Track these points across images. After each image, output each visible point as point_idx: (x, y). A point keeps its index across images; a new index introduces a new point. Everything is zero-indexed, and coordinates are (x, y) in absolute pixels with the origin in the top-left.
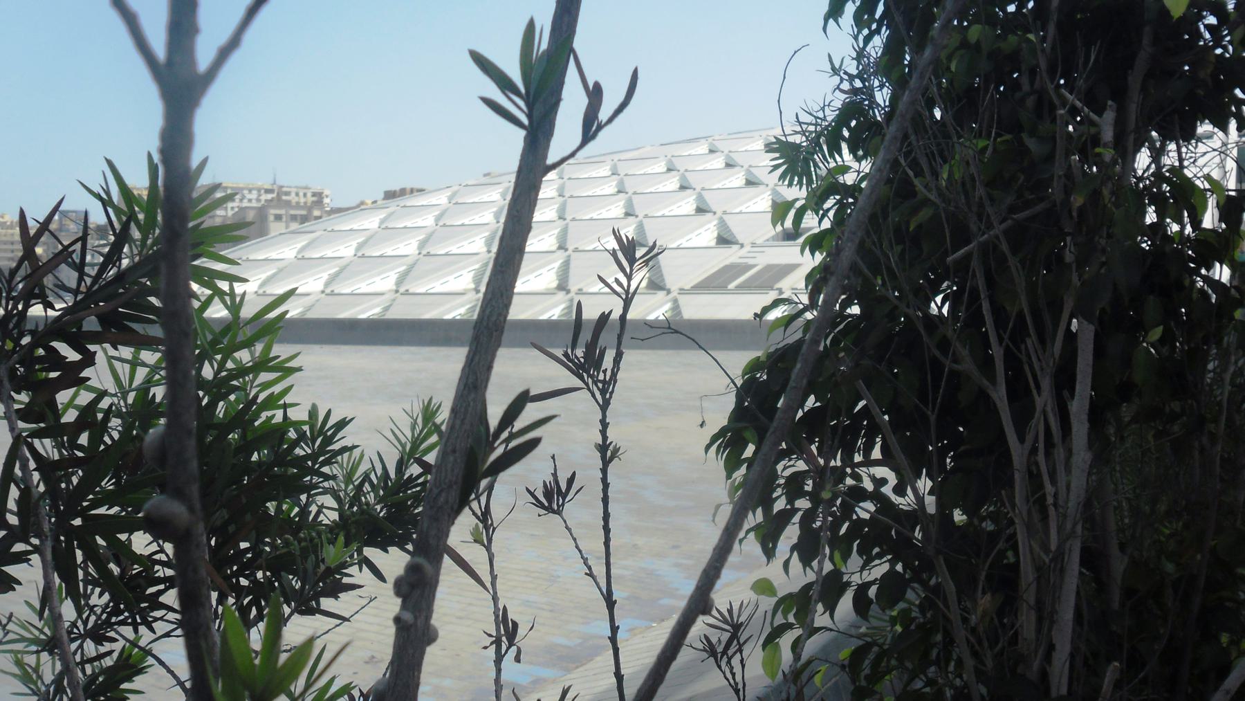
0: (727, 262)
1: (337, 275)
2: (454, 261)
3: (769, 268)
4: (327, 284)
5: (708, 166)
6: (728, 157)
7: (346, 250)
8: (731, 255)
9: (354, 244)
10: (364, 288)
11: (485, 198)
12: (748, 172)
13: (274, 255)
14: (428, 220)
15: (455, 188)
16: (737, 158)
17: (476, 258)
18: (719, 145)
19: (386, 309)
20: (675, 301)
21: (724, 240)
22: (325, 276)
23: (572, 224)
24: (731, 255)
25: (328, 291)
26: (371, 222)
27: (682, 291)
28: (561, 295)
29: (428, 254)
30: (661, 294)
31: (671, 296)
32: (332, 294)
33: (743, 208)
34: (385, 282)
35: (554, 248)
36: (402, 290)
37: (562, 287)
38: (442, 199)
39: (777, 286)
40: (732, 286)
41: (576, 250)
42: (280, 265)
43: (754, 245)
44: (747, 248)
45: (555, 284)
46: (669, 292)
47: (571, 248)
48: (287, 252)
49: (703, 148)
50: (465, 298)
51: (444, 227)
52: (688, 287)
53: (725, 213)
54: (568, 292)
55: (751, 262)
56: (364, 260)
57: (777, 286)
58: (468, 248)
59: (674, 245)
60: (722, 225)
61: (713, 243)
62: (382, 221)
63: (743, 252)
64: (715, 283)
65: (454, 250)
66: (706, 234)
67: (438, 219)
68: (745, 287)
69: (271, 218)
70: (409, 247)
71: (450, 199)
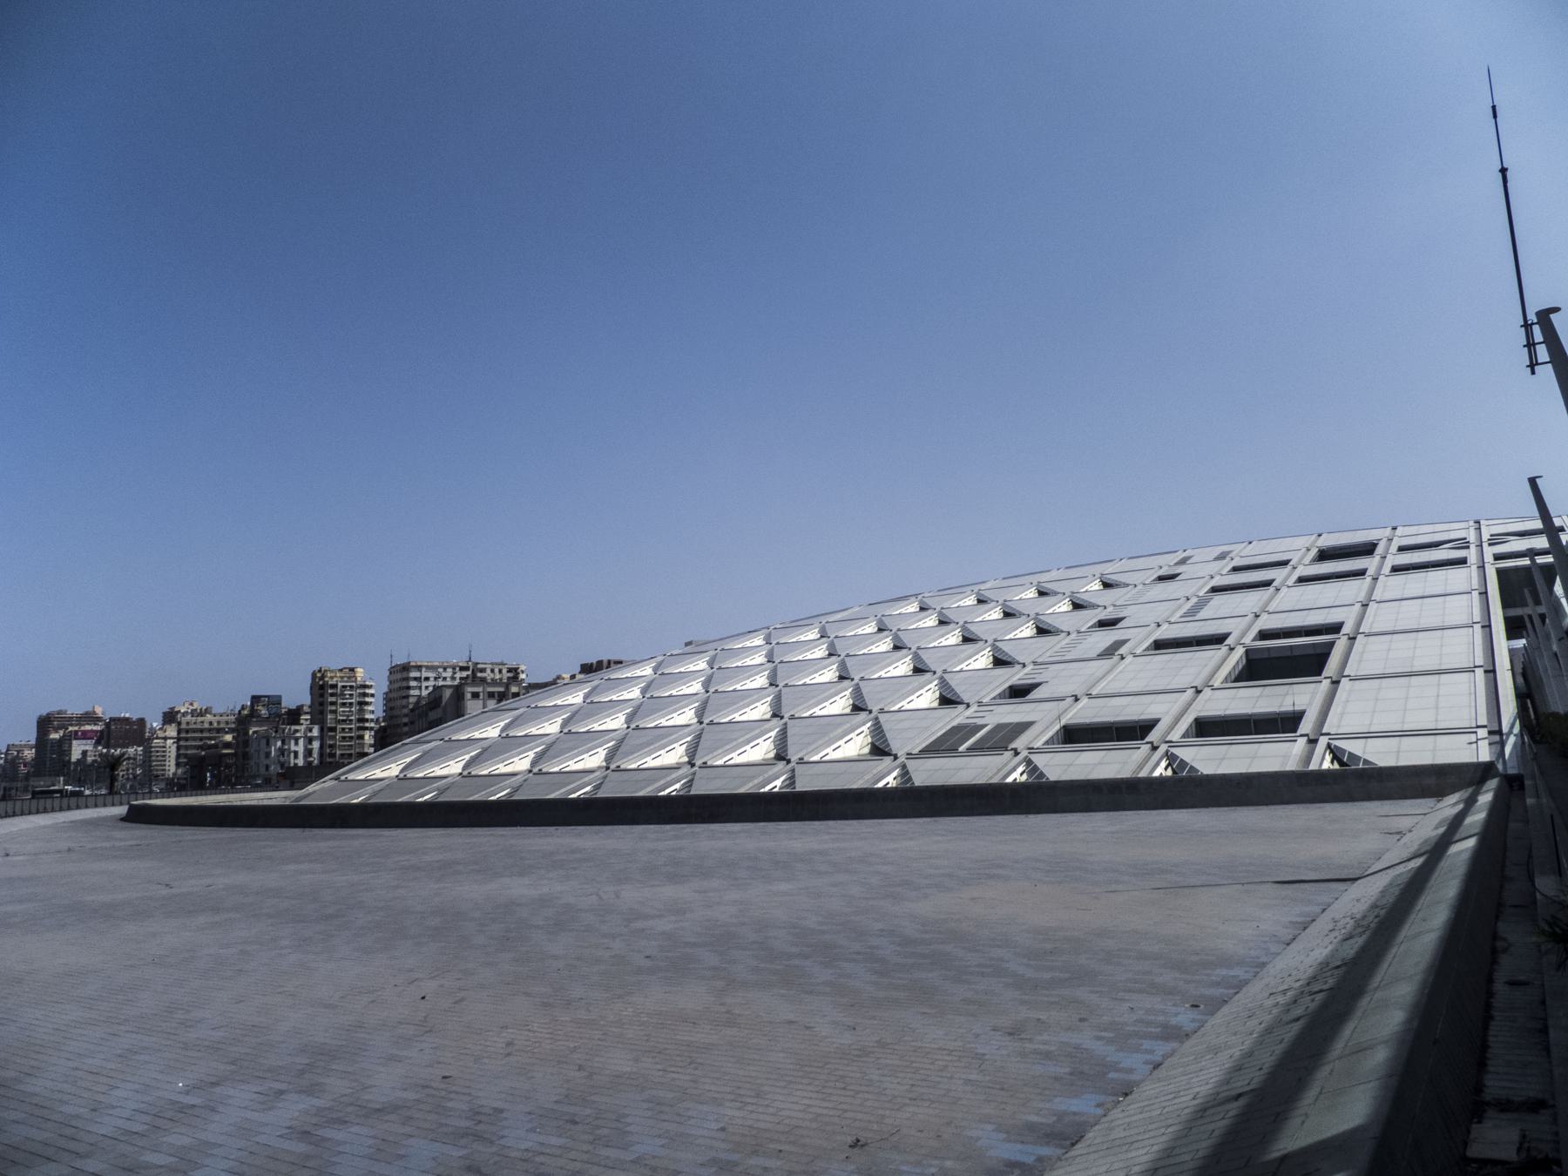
0: (955, 723)
1: (543, 753)
2: (664, 736)
3: (999, 727)
4: (534, 763)
5: (921, 624)
6: (940, 614)
7: (552, 727)
8: (957, 716)
9: (559, 720)
10: (573, 765)
11: (692, 668)
12: (964, 628)
13: (477, 735)
14: (634, 693)
15: (660, 658)
16: (951, 615)
17: (687, 730)
18: (929, 602)
19: (597, 788)
20: (904, 767)
21: (947, 700)
22: (531, 754)
23: (784, 691)
24: (957, 716)
25: (536, 770)
26: (576, 698)
27: (910, 756)
28: (781, 764)
29: (637, 728)
30: (888, 760)
31: (898, 762)
32: (540, 773)
33: (963, 666)
34: (594, 760)
35: (768, 716)
36: (613, 766)
37: (781, 756)
38: (647, 671)
39: (1013, 745)
40: (961, 749)
41: (792, 717)
42: (485, 744)
43: (980, 704)
44: (974, 708)
45: (772, 755)
46: (896, 757)
47: (787, 716)
48: (492, 732)
49: (913, 607)
50: (681, 772)
51: (652, 702)
52: (916, 751)
53: (945, 671)
54: (789, 762)
55: (980, 722)
56: (571, 739)
57: (1013, 745)
58: (678, 719)
59: (896, 708)
60: (943, 684)
61: (936, 704)
62: (586, 696)
63: (970, 712)
64: (944, 746)
65: (664, 722)
66: (926, 697)
67: (644, 691)
68: (976, 749)
69: (469, 696)
70: (616, 722)
71: (655, 670)
